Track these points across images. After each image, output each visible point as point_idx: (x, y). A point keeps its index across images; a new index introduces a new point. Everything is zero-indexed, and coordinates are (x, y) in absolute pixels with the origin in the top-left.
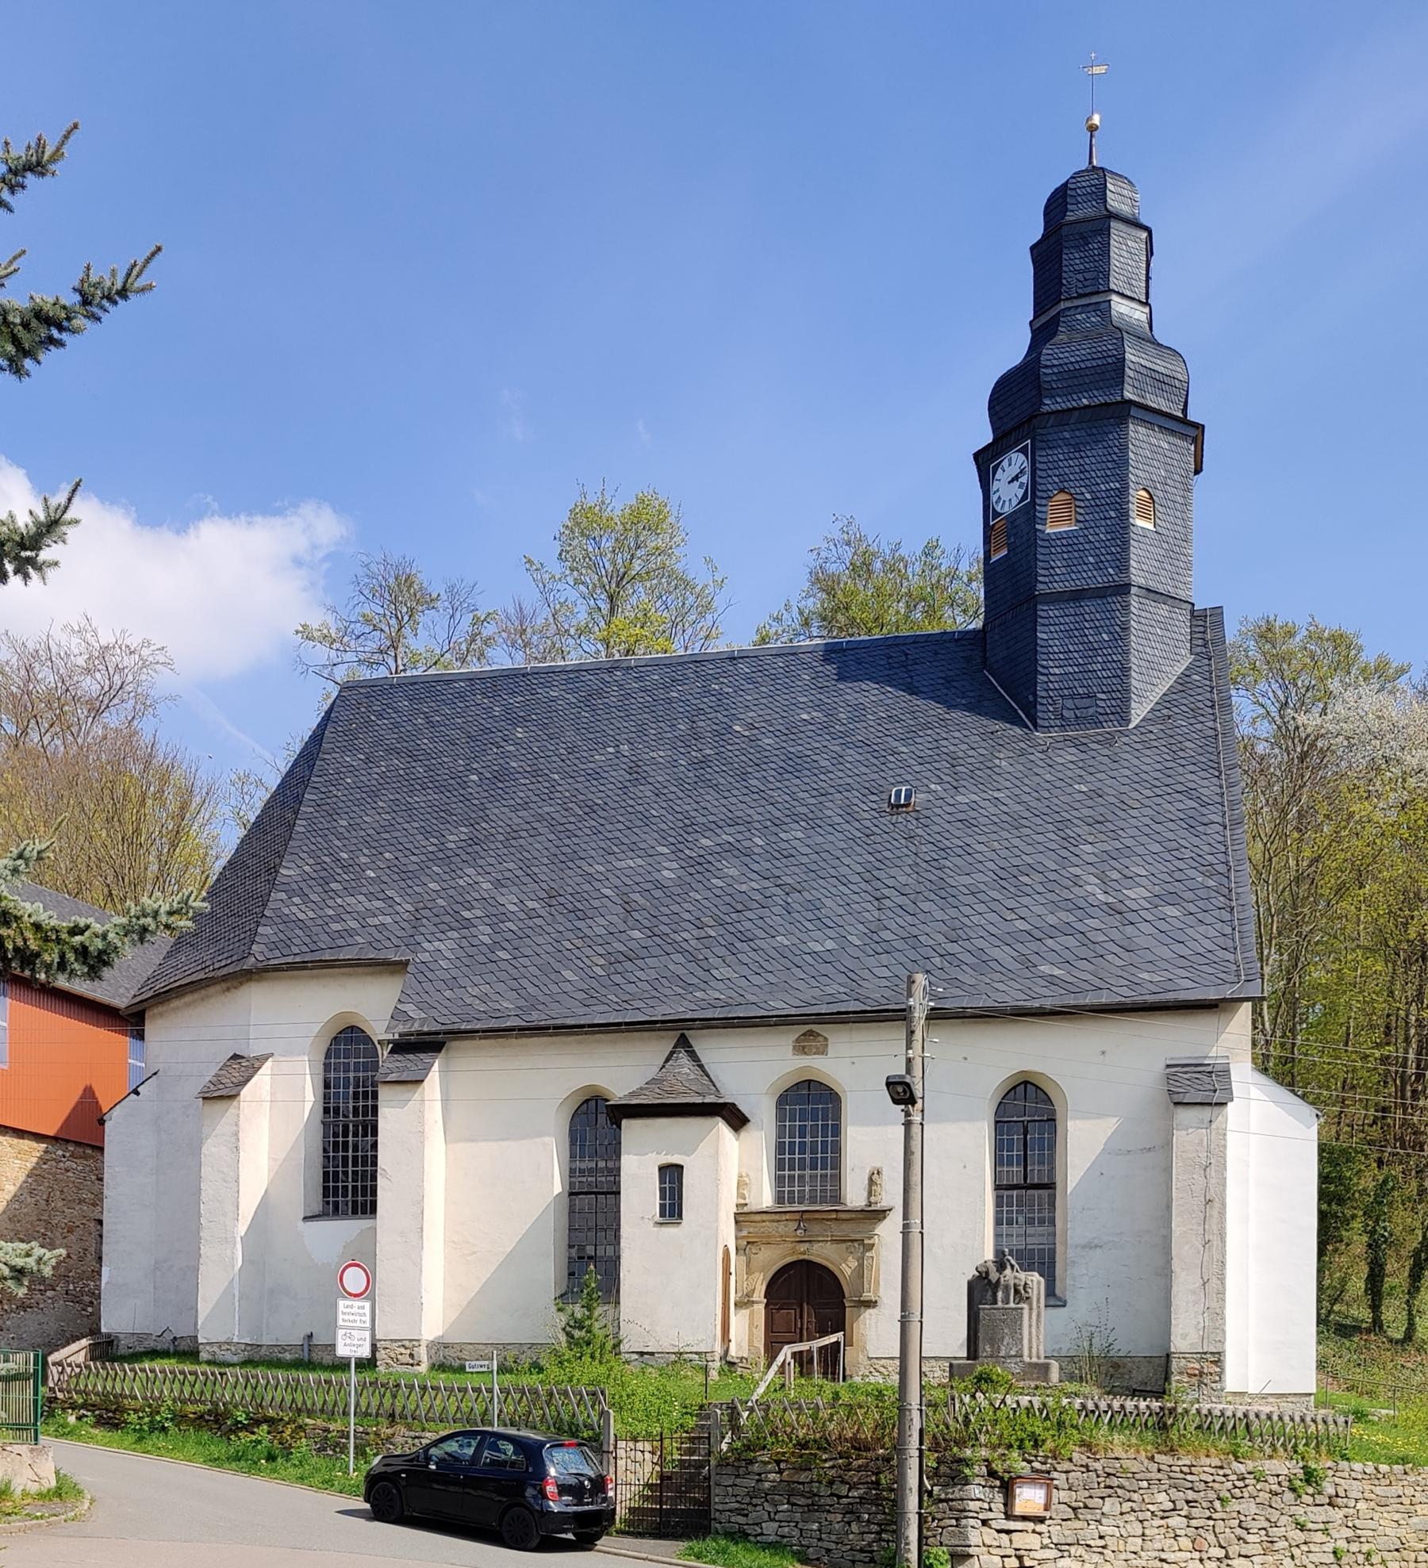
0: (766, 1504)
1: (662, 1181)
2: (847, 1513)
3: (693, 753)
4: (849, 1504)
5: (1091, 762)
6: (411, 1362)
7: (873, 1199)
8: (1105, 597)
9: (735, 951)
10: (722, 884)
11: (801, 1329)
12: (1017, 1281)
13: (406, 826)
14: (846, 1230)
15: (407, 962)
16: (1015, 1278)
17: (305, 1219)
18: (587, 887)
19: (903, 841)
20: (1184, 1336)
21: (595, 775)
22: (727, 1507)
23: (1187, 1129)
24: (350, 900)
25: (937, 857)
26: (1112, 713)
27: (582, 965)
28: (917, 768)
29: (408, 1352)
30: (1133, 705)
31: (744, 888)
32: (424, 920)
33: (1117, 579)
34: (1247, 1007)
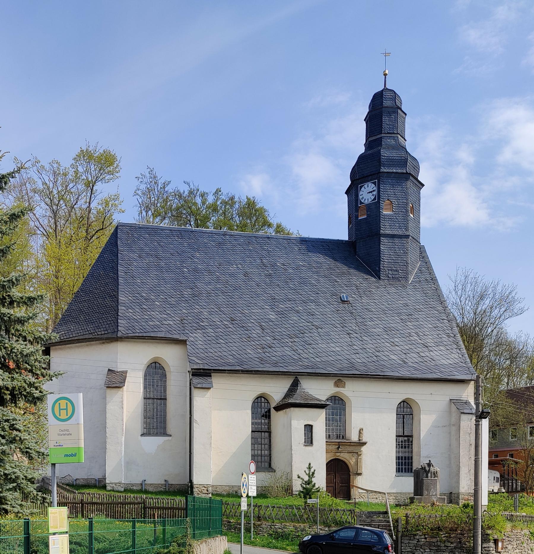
0: (421, 549)
2: (451, 552)
3: (266, 272)
4: (451, 549)
5: (401, 293)
6: (207, 493)
7: (360, 438)
8: (402, 238)
9: (307, 348)
10: (293, 323)
11: (336, 482)
12: (435, 470)
13: (165, 286)
14: (351, 449)
15: (186, 341)
16: (434, 469)
17: (142, 435)
18: (244, 318)
19: (350, 314)
20: (463, 488)
21: (232, 275)
22: (407, 550)
23: (464, 421)
24: (152, 313)
25: (363, 321)
26: (404, 278)
27: (253, 348)
28: (346, 288)
29: (206, 489)
30: (410, 276)
31: (301, 325)
32: (186, 324)
33: (405, 233)
34: (473, 382)
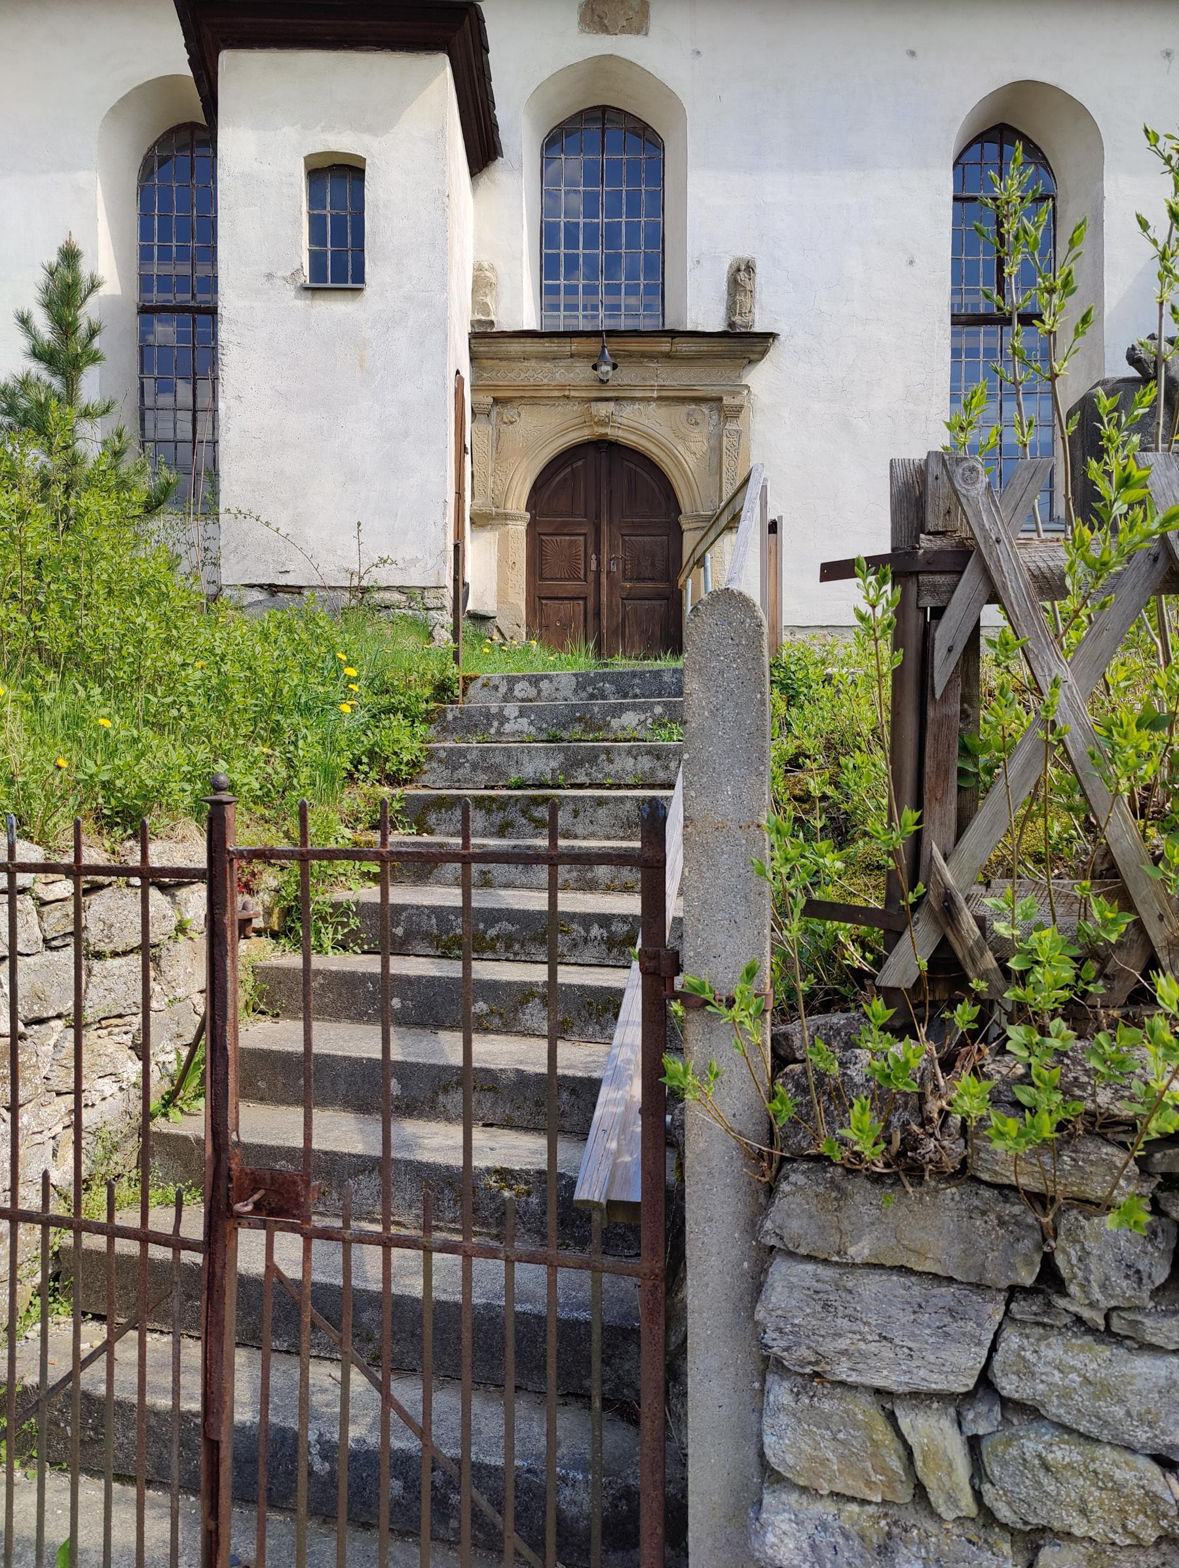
1: (315, 200)
11: (598, 573)
